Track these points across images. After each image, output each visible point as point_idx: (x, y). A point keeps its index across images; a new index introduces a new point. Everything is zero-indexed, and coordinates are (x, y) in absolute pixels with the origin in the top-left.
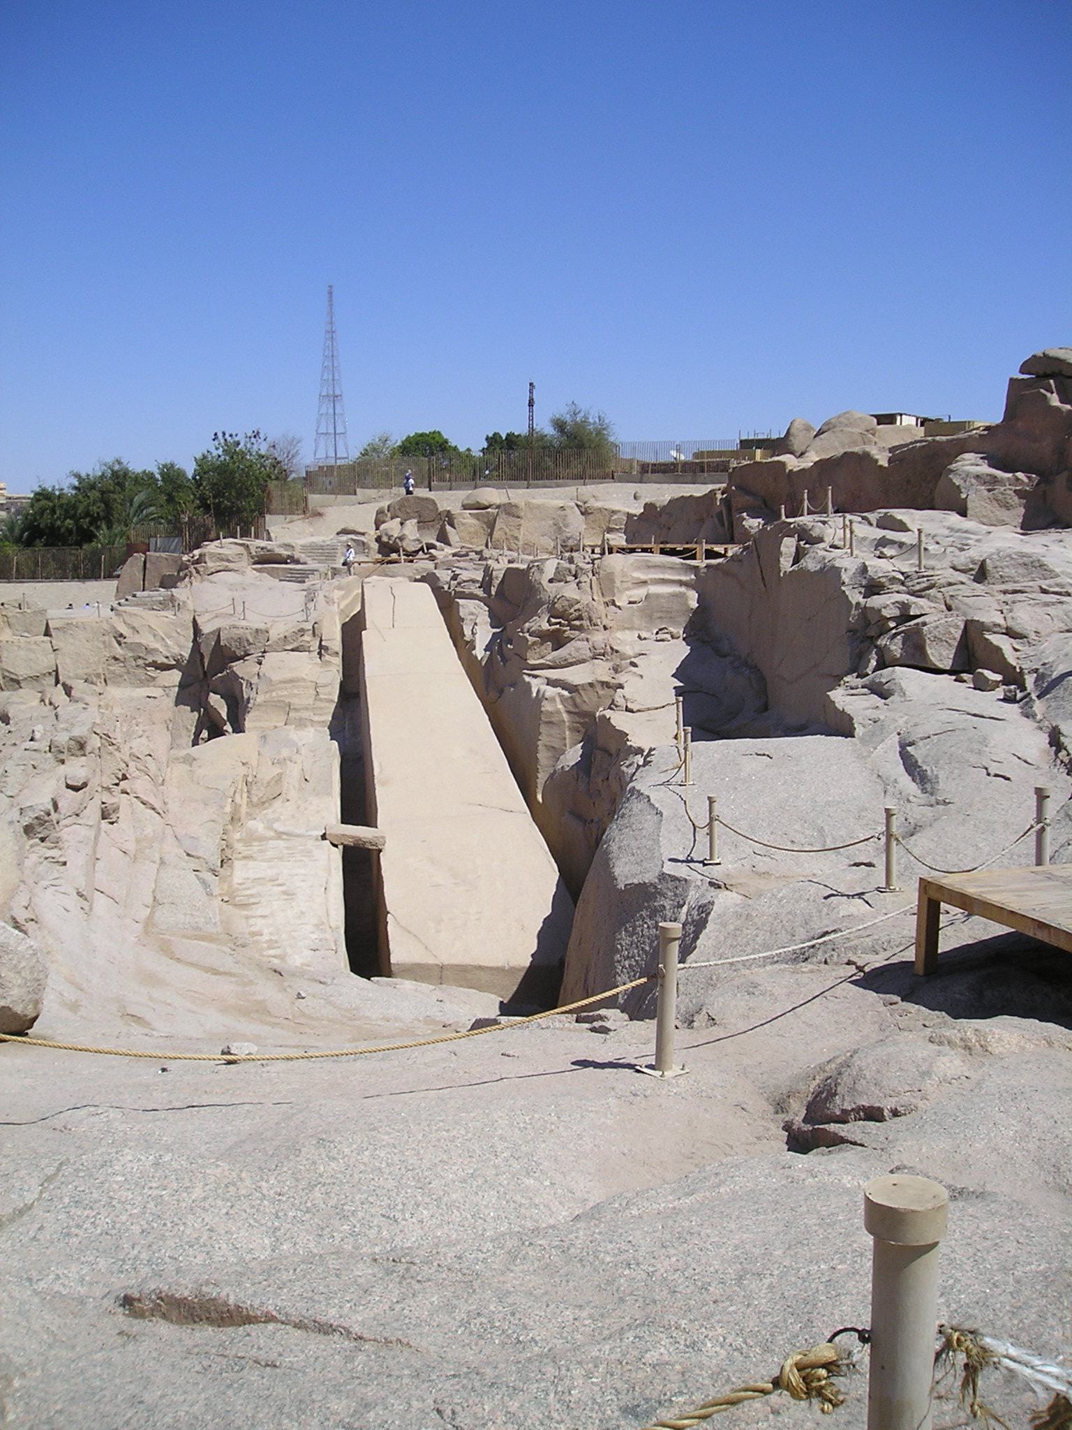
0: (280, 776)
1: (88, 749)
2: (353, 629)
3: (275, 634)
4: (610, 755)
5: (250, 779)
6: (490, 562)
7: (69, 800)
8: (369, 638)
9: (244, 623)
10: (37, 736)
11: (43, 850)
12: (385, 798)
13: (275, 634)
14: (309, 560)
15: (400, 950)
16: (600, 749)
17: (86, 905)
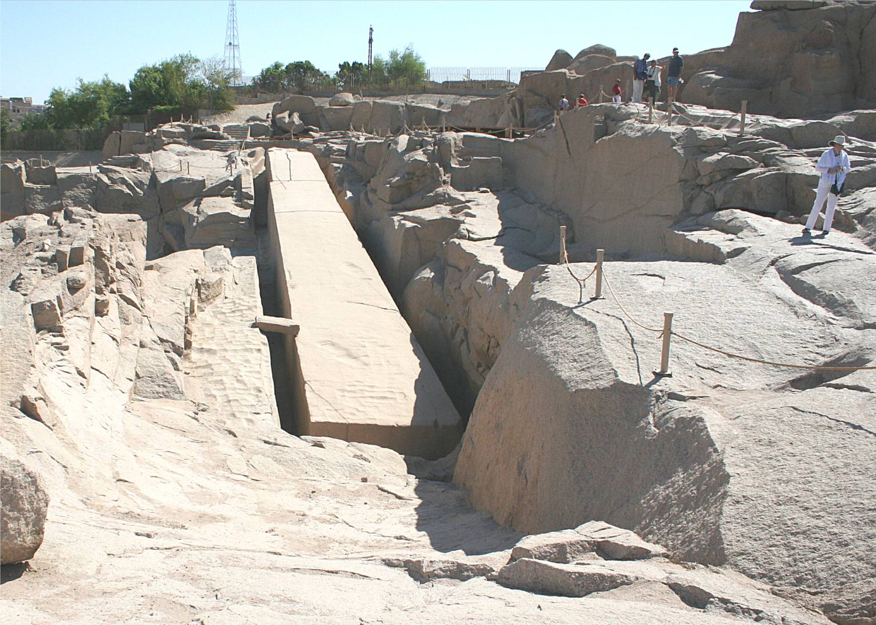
0: (221, 280)
1: (85, 258)
2: (263, 183)
3: (208, 184)
4: (460, 271)
5: (200, 282)
6: (353, 139)
7: (68, 300)
8: (275, 188)
9: (188, 177)
10: (46, 247)
11: (50, 338)
12: (296, 296)
13: (208, 184)
14: (229, 137)
15: (318, 412)
16: (450, 266)
17: (84, 381)
